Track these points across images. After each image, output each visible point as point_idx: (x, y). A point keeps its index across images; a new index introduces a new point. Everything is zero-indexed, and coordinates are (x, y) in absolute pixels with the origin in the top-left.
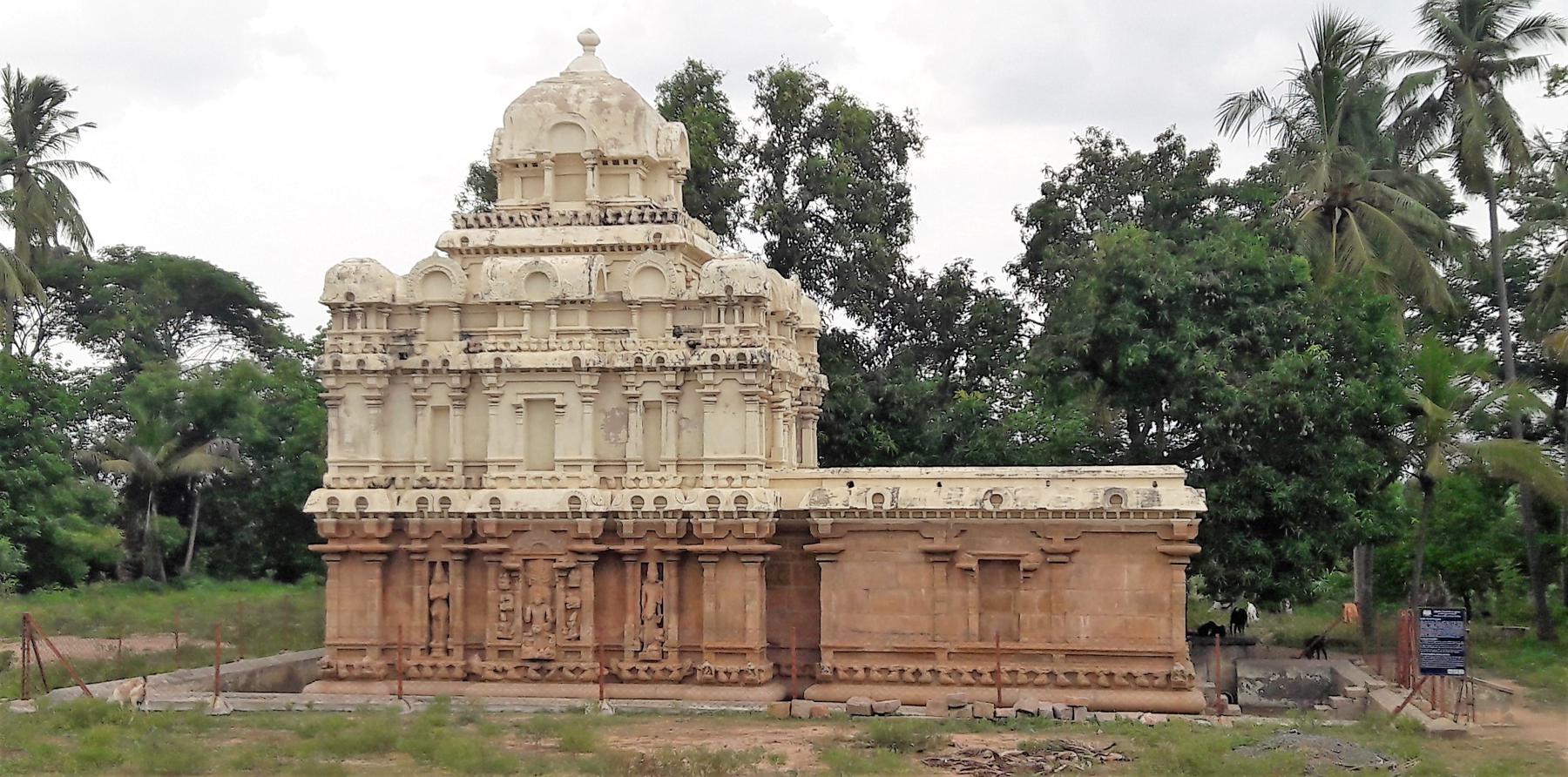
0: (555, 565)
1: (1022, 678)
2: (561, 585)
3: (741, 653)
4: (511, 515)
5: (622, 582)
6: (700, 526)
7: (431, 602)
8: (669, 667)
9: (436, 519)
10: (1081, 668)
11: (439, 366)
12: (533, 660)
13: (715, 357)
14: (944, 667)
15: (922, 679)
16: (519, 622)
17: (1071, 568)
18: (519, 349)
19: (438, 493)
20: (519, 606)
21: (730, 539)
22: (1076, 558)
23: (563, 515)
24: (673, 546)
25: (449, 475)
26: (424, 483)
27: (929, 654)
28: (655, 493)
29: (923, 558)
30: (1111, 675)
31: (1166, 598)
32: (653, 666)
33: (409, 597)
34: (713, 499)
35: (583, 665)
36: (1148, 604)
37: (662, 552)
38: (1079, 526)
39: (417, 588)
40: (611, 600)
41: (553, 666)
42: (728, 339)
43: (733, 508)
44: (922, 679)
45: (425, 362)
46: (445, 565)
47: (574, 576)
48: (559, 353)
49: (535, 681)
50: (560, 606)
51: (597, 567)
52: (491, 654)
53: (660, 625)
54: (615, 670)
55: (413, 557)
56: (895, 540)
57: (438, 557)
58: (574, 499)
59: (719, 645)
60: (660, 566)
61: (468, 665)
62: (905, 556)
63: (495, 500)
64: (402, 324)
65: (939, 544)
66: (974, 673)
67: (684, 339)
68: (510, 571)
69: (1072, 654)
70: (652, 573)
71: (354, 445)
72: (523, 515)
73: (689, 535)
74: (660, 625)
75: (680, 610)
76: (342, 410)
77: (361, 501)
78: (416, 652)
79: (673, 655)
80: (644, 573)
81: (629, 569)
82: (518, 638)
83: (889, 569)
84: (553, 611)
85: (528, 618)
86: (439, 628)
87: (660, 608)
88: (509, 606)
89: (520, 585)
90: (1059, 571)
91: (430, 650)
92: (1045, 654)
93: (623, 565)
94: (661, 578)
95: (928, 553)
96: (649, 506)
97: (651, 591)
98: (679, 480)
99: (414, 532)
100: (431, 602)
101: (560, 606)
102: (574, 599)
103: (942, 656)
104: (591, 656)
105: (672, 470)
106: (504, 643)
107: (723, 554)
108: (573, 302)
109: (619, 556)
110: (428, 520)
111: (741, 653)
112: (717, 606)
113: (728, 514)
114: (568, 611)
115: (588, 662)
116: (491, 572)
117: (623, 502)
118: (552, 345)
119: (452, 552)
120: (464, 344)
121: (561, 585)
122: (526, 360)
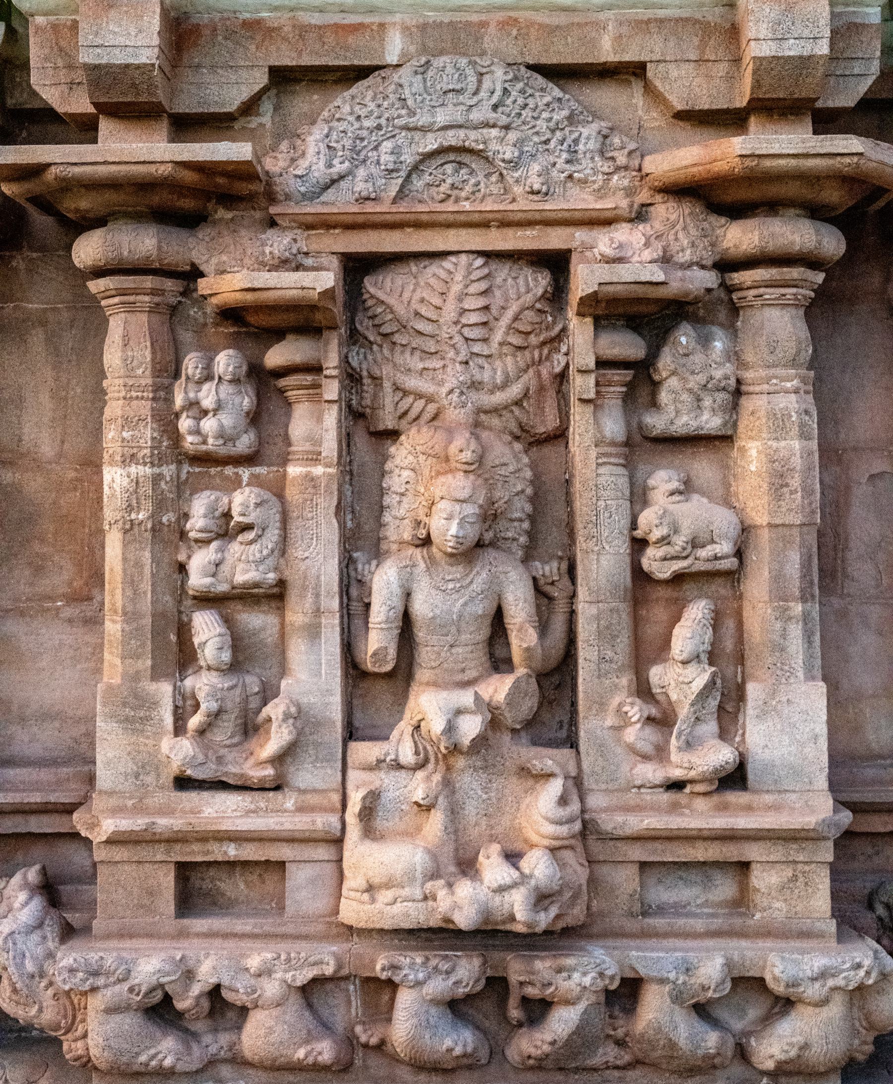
2: (593, 431)
50: (602, 564)
68: (252, 323)
82: (311, 775)
88: (245, 564)
89: (315, 426)
101: (602, 564)
106: (222, 810)
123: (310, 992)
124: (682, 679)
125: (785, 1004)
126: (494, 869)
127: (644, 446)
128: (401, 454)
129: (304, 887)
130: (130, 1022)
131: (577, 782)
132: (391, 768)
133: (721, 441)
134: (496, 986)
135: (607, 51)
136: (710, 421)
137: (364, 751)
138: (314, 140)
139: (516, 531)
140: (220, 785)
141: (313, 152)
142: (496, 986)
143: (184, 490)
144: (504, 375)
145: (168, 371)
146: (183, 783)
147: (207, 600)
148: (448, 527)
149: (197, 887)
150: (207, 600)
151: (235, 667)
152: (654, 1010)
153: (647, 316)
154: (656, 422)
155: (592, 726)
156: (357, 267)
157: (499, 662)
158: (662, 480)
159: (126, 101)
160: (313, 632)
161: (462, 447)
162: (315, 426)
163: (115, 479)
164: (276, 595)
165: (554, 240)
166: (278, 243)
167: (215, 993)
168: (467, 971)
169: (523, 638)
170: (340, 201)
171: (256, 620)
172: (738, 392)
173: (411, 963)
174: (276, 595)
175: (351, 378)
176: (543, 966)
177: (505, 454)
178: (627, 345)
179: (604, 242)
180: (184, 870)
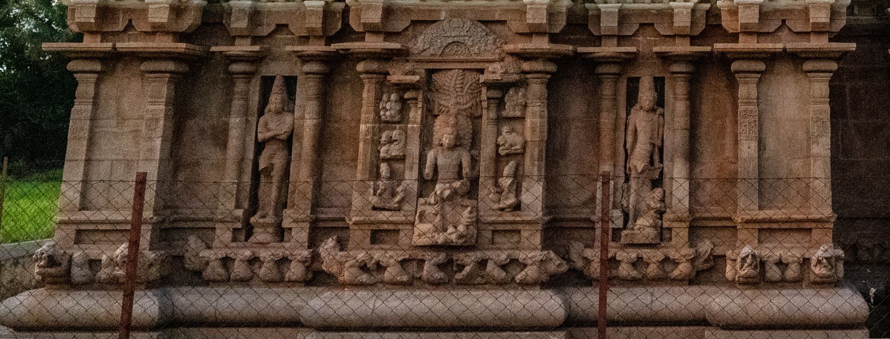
0: (482, 78)
2: (487, 116)
5: (594, 110)
7: (260, 147)
8: (673, 254)
16: (411, 178)
20: (414, 149)
24: (682, 47)
32: (646, 253)
35: (521, 256)
37: (666, 58)
39: (235, 121)
40: (576, 138)
46: (290, 83)
51: (554, 87)
53: (657, 183)
54: (580, 264)
57: (277, 69)
60: (659, 84)
70: (646, 95)
74: (657, 183)
75: (692, 157)
81: (607, 90)
84: (474, 161)
85: (428, 170)
88: (395, 150)
89: (416, 114)
93: (598, 82)
94: (660, 102)
100: (260, 147)
101: (487, 151)
102: (510, 138)
104: (537, 239)
109: (591, 64)
114: (498, 159)
115: (531, 251)
116: (368, 94)
121: (487, 116)
124: (506, 182)
127: (500, 120)
162: (416, 114)
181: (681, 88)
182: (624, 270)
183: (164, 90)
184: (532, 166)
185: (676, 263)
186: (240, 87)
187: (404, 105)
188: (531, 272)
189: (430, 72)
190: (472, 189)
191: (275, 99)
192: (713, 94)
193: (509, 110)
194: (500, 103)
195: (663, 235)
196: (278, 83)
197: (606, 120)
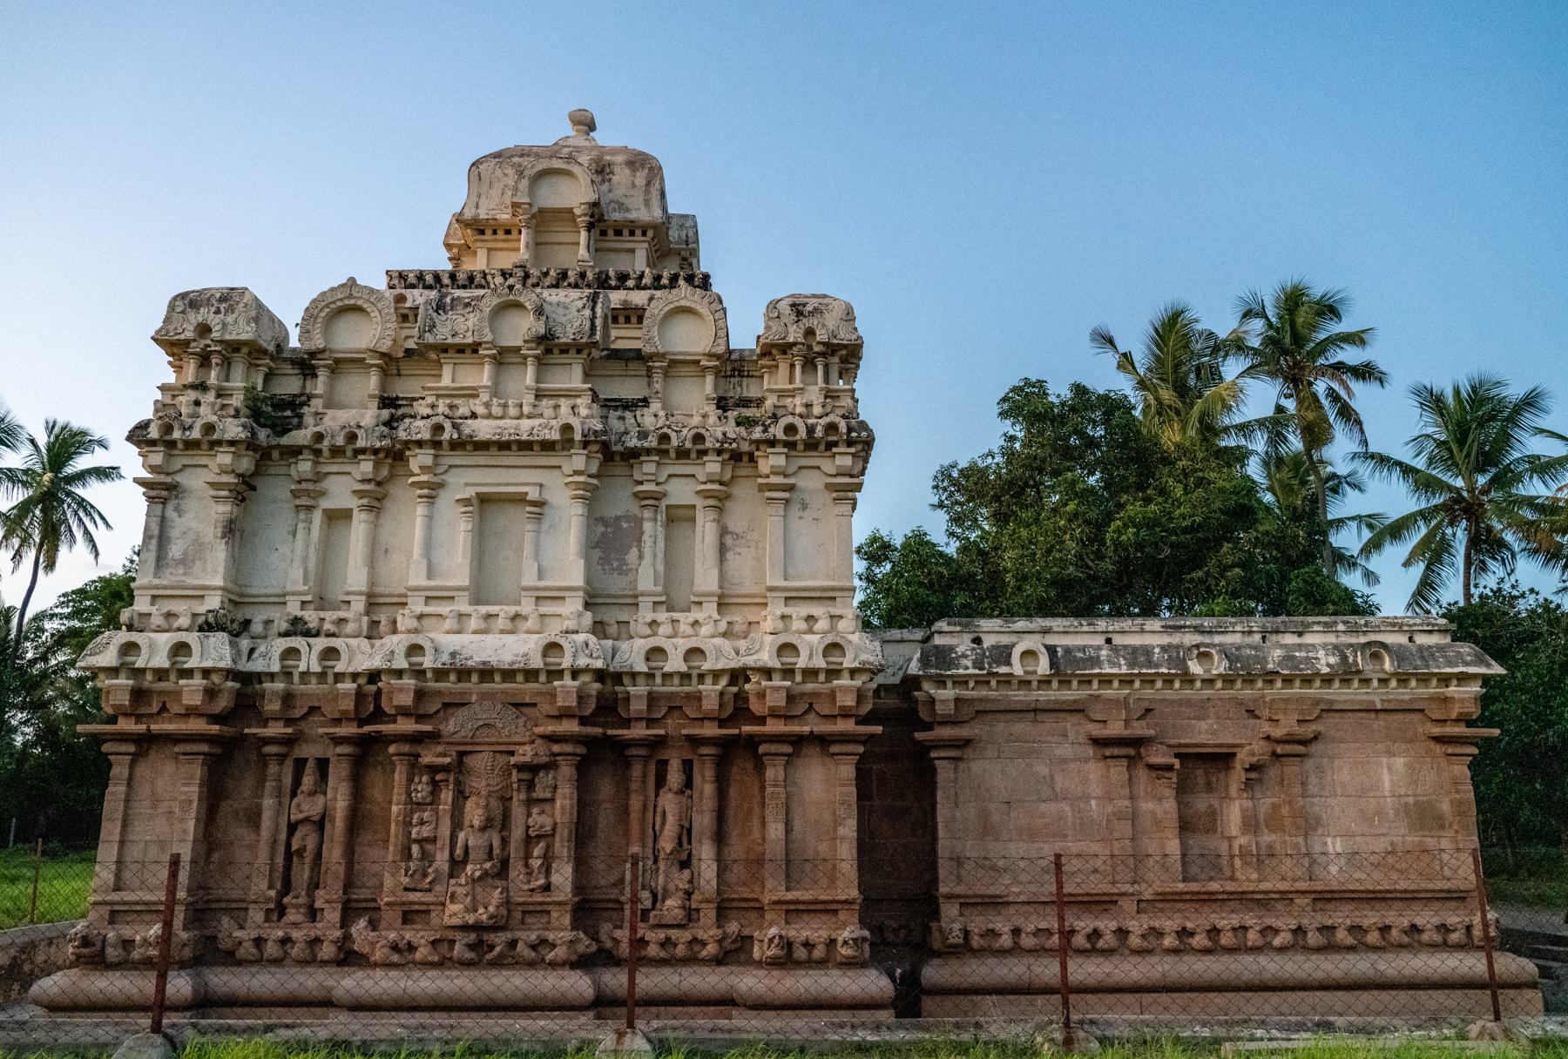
0: (513, 760)
1: (1253, 937)
2: (518, 797)
3: (826, 909)
4: (440, 674)
5: (624, 791)
6: (761, 695)
8: (701, 935)
9: (313, 686)
10: (1341, 917)
11: (340, 441)
12: (465, 928)
13: (791, 429)
14: (1136, 926)
15: (1101, 944)
16: (442, 860)
17: (1309, 764)
18: (474, 416)
19: (320, 643)
20: (445, 830)
21: (811, 716)
22: (1314, 748)
23: (531, 674)
24: (710, 730)
25: (342, 614)
26: (297, 627)
27: (1101, 903)
28: (684, 644)
29: (1090, 751)
30: (1385, 930)
31: (1445, 807)
32: (674, 934)
33: (254, 818)
34: (787, 648)
35: (551, 936)
36: (1423, 816)
37: (695, 742)
38: (1317, 702)
39: (268, 802)
40: (605, 817)
41: (500, 940)
42: (808, 406)
43: (820, 662)
44: (1101, 944)
45: (319, 437)
46: (323, 765)
47: (544, 780)
48: (537, 422)
49: (468, 964)
50: (517, 833)
51: (584, 768)
52: (390, 916)
53: (685, 864)
54: (608, 944)
55: (268, 749)
56: (1049, 724)
57: (310, 751)
58: (552, 648)
59: (790, 896)
60: (687, 766)
61: (347, 937)
62: (1065, 750)
63: (415, 649)
64: (289, 386)
65: (1115, 729)
66: (1184, 933)
67: (732, 414)
68: (433, 769)
69: (1325, 898)
70: (674, 777)
71: (185, 561)
72: (464, 674)
73: (739, 709)
74: (685, 864)
75: (720, 838)
76: (170, 506)
77: (181, 649)
78: (256, 915)
79: (709, 915)
80: (661, 782)
81: (636, 771)
82: (438, 888)
83: (1043, 770)
84: (505, 842)
85: (459, 851)
86: (302, 873)
87: (685, 833)
88: (426, 831)
89: (447, 796)
90: (1292, 769)
91: (281, 910)
92: (1286, 897)
93: (627, 764)
94: (689, 784)
95: (1098, 742)
96: (675, 663)
97: (669, 802)
98: (723, 626)
99: (273, 706)
101: (517, 833)
102: (540, 820)
103: (1128, 905)
104: (567, 920)
105: (711, 609)
107: (798, 741)
108: (564, 350)
109: (621, 745)
110: (298, 687)
111: (826, 909)
112: (788, 829)
113: (810, 673)
114: (529, 841)
115: (561, 931)
116: (399, 775)
117: (633, 654)
118: (526, 410)
119: (337, 741)
120: (386, 413)
121: (518, 797)
122: (484, 429)
123: (434, 943)
124: (536, 863)
125: (554, 946)
126: (481, 910)
127: (530, 802)
128: (469, 804)
129: (434, 919)
130: (386, 950)
131: (506, 890)
132: (460, 886)
133: (552, 800)
134: (480, 942)
135: (527, 700)
136: (548, 795)
137: (453, 881)
138: (452, 722)
139: (498, 823)
140: (415, 890)
141: (451, 725)
142: (480, 942)
143: (412, 812)
144: (496, 782)
145: (410, 780)
146: (406, 889)
147: (416, 841)
148: (476, 823)
149: (409, 917)
150: (416, 841)
151: (422, 859)
152: (520, 946)
153: (532, 769)
154: (534, 795)
155: (512, 874)
156: (462, 754)
157: (490, 858)
158: (535, 810)
159: (404, 712)
160: (442, 849)
161: (483, 802)
162: (447, 796)
163: (394, 808)
164: (434, 840)
165: (511, 748)
166: (440, 749)
167: (409, 943)
168: (473, 936)
169: (496, 851)
170: (457, 738)
171: (429, 847)
172: (556, 788)
173: (458, 936)
174: (434, 840)
175: (458, 783)
176: (492, 936)
177: (494, 803)
178: (525, 776)
179: (521, 750)
180: (405, 913)
181: (709, 772)
182: (653, 950)
183: (197, 771)
184: (562, 848)
185: (704, 944)
186: (273, 768)
187: (435, 786)
188: (560, 953)
189: (462, 754)
190: (503, 870)
191: (308, 781)
192: (740, 771)
193: (540, 793)
194: (531, 786)
195: (691, 916)
196: (310, 765)
197: (635, 802)
